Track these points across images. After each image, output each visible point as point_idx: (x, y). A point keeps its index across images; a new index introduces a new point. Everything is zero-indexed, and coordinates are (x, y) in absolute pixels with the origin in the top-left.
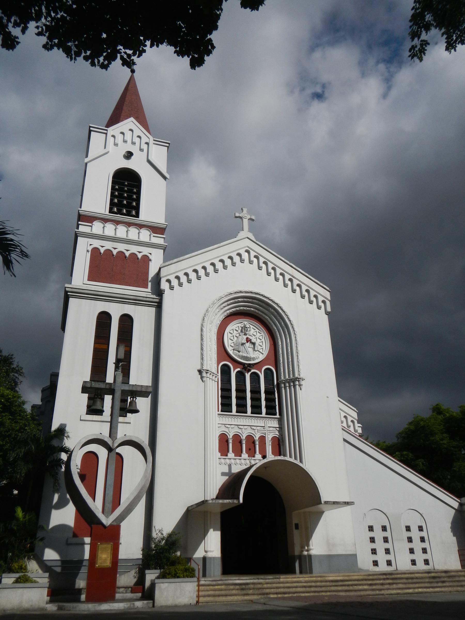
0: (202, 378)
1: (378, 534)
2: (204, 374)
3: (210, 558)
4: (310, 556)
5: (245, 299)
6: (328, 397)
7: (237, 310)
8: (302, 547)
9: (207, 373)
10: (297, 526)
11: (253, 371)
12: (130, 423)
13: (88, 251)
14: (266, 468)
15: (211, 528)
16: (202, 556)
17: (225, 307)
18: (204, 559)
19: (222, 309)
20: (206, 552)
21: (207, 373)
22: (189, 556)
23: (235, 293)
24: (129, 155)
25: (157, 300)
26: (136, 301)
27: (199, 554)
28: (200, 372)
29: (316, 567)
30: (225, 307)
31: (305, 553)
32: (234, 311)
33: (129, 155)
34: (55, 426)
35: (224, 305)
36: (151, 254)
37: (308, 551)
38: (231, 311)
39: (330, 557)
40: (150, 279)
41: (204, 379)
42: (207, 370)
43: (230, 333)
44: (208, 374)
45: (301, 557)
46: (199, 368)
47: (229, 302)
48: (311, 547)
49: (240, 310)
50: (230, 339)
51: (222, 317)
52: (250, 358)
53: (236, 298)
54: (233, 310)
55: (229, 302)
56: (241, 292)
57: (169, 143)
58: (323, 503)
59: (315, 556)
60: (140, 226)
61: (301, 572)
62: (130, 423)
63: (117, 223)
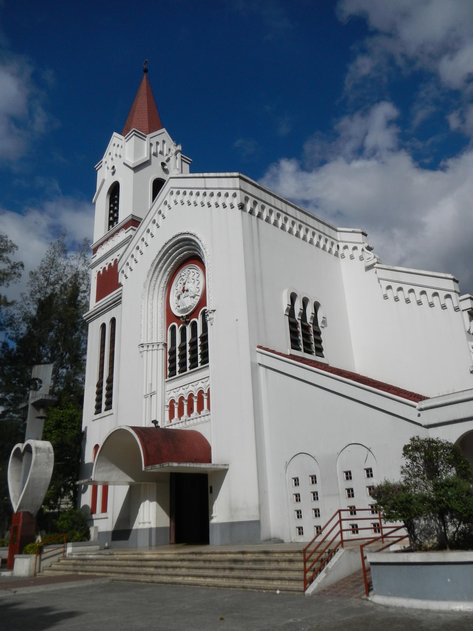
1: (306, 489)
5: (173, 248)
6: (237, 320)
7: (176, 263)
11: (191, 321)
12: (112, 414)
15: (144, 500)
17: (162, 268)
19: (160, 271)
23: (163, 248)
30: (162, 268)
32: (174, 265)
34: (83, 429)
35: (159, 266)
39: (232, 525)
42: (142, 344)
49: (178, 260)
51: (166, 278)
52: (187, 308)
53: (166, 253)
54: (172, 264)
55: (162, 262)
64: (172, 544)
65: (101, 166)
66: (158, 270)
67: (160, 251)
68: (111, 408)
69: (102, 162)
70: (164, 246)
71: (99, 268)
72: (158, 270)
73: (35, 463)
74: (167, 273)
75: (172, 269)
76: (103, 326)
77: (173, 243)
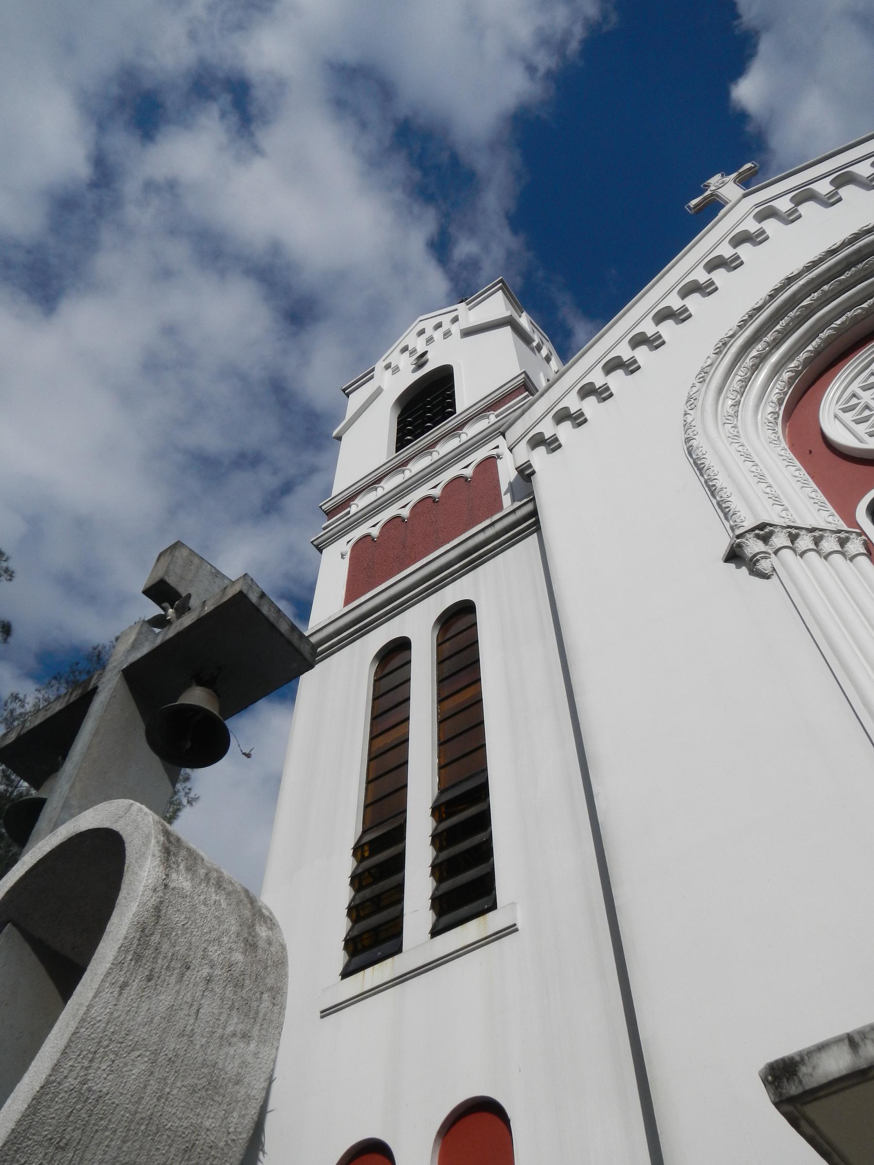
0: (752, 566)
2: (753, 546)
5: (826, 288)
7: (829, 341)
9: (766, 539)
12: (512, 929)
13: (343, 556)
19: (756, 368)
21: (766, 539)
24: (421, 360)
25: (529, 508)
26: (472, 559)
28: (734, 556)
30: (762, 358)
32: (818, 352)
33: (421, 360)
36: (497, 447)
38: (803, 356)
40: (504, 486)
41: (764, 565)
42: (762, 526)
43: (845, 410)
44: (780, 539)
46: (723, 545)
47: (769, 338)
50: (858, 422)
54: (810, 348)
55: (769, 338)
56: (790, 280)
57: (501, 281)
60: (461, 426)
62: (512, 929)
63: (405, 463)
65: (372, 377)
66: (748, 362)
67: (759, 309)
68: (493, 907)
69: (373, 370)
70: (777, 291)
71: (371, 528)
72: (748, 362)
73: (143, 930)
74: (786, 376)
75: (807, 362)
76: (396, 652)
77: (829, 269)
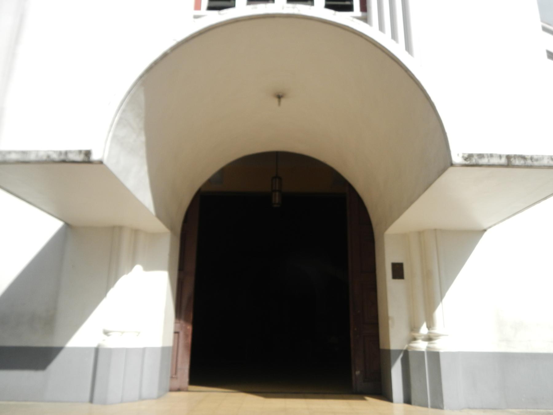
3: (110, 351)
4: (435, 356)
8: (414, 328)
10: (398, 271)
14: (279, 97)
16: (95, 345)
18: (97, 350)
20: (106, 333)
22: (56, 344)
27: (84, 337)
29: (453, 385)
31: (421, 346)
37: (429, 339)
45: (406, 356)
48: (438, 329)
58: (457, 158)
59: (454, 355)
61: (408, 400)
64: (179, 390)
